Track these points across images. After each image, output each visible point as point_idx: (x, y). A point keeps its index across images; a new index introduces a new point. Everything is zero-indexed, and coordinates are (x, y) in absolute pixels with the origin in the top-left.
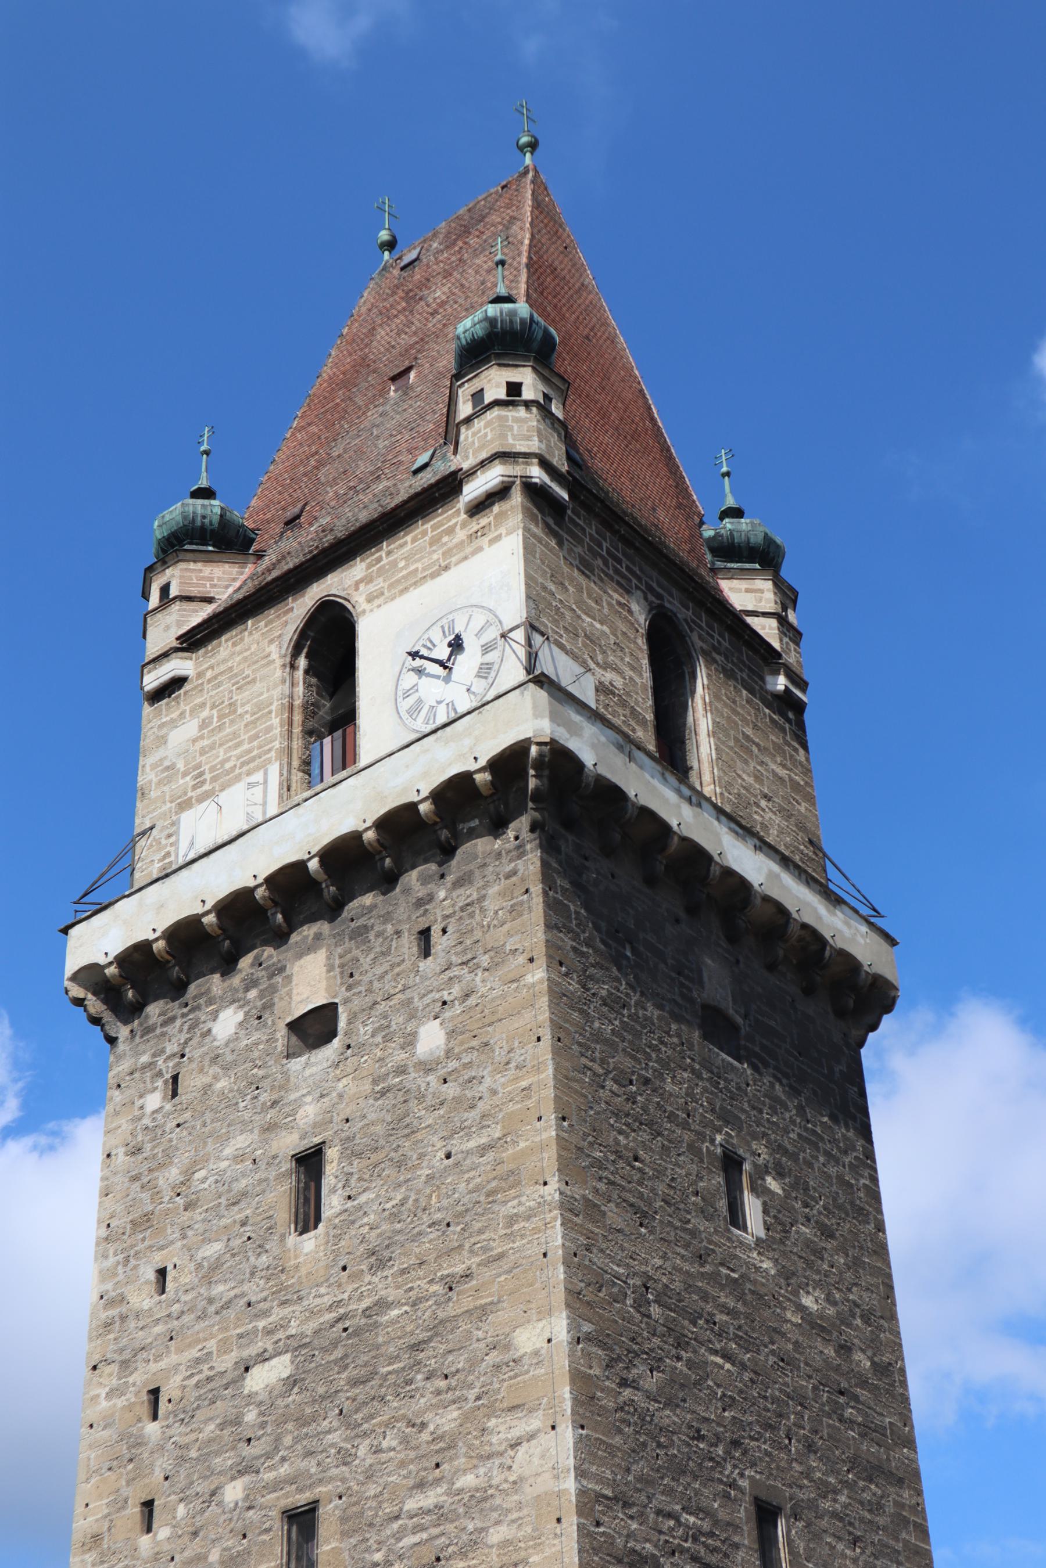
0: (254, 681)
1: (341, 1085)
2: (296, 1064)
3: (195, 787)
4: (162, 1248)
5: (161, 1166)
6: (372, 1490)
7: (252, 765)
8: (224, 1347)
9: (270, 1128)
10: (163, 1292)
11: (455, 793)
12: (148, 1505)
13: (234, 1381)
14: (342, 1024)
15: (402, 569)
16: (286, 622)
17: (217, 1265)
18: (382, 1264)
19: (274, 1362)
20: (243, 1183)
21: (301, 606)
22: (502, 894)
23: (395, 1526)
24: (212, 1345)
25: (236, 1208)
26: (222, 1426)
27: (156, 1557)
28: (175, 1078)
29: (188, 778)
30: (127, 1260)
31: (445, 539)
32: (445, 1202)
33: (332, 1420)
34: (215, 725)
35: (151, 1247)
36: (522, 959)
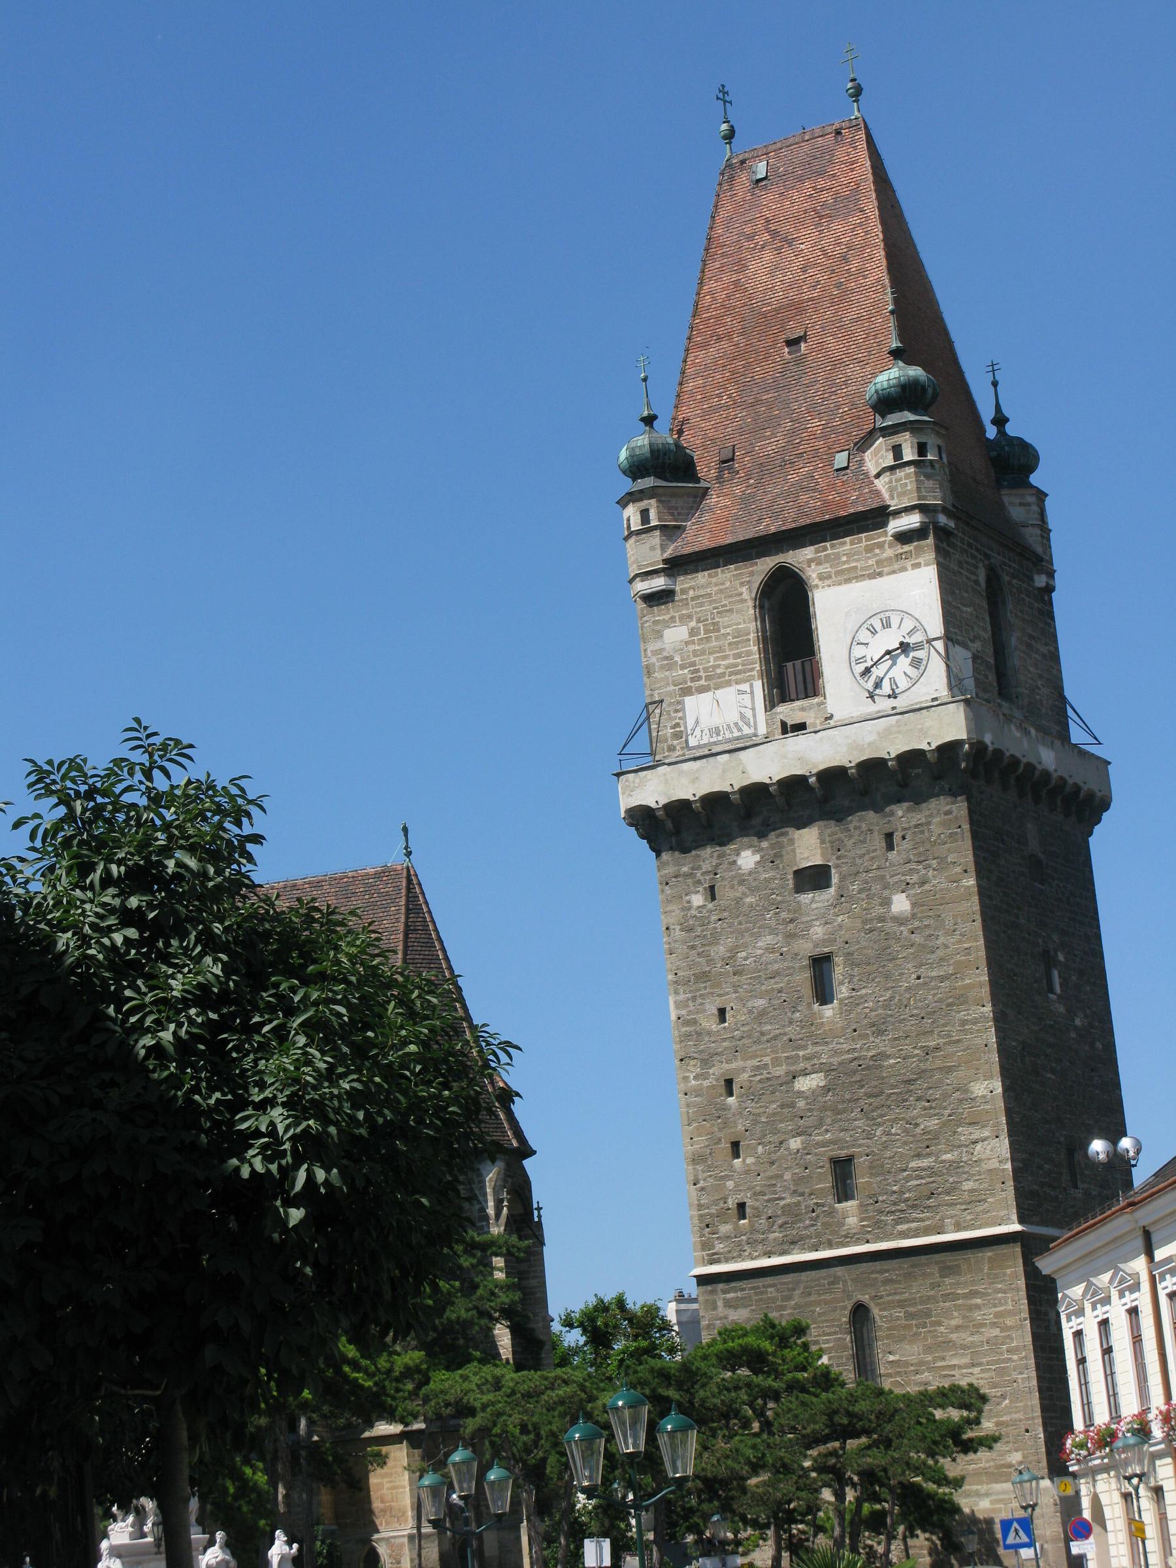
0: (731, 611)
1: (840, 919)
2: (806, 898)
3: (692, 680)
4: (720, 995)
5: (710, 944)
6: (888, 1154)
7: (739, 677)
8: (776, 1062)
9: (790, 936)
10: (722, 1019)
11: (912, 758)
12: (735, 1146)
13: (787, 1083)
14: (835, 879)
15: (845, 563)
16: (752, 574)
17: (763, 1013)
18: (880, 1033)
19: (813, 1076)
20: (776, 966)
21: (765, 565)
22: (943, 824)
23: (905, 1174)
24: (767, 1060)
25: (773, 981)
26: (782, 1106)
27: (747, 1172)
28: (712, 888)
29: (686, 671)
30: (694, 999)
31: (877, 551)
32: (920, 1004)
33: (856, 1113)
34: (702, 636)
35: (712, 993)
36: (958, 869)
